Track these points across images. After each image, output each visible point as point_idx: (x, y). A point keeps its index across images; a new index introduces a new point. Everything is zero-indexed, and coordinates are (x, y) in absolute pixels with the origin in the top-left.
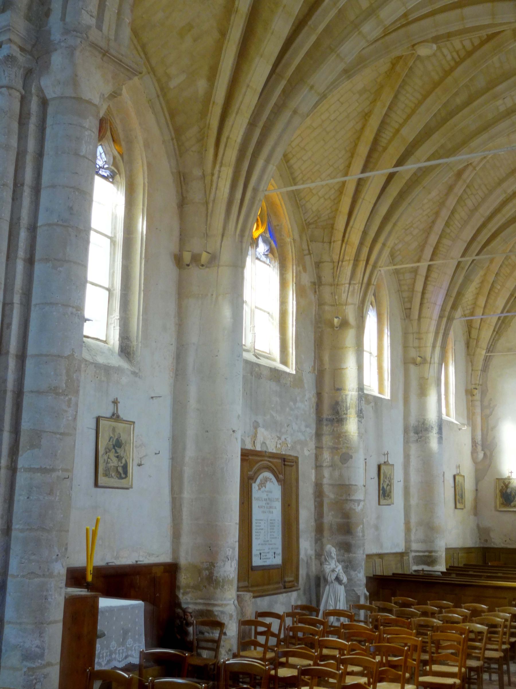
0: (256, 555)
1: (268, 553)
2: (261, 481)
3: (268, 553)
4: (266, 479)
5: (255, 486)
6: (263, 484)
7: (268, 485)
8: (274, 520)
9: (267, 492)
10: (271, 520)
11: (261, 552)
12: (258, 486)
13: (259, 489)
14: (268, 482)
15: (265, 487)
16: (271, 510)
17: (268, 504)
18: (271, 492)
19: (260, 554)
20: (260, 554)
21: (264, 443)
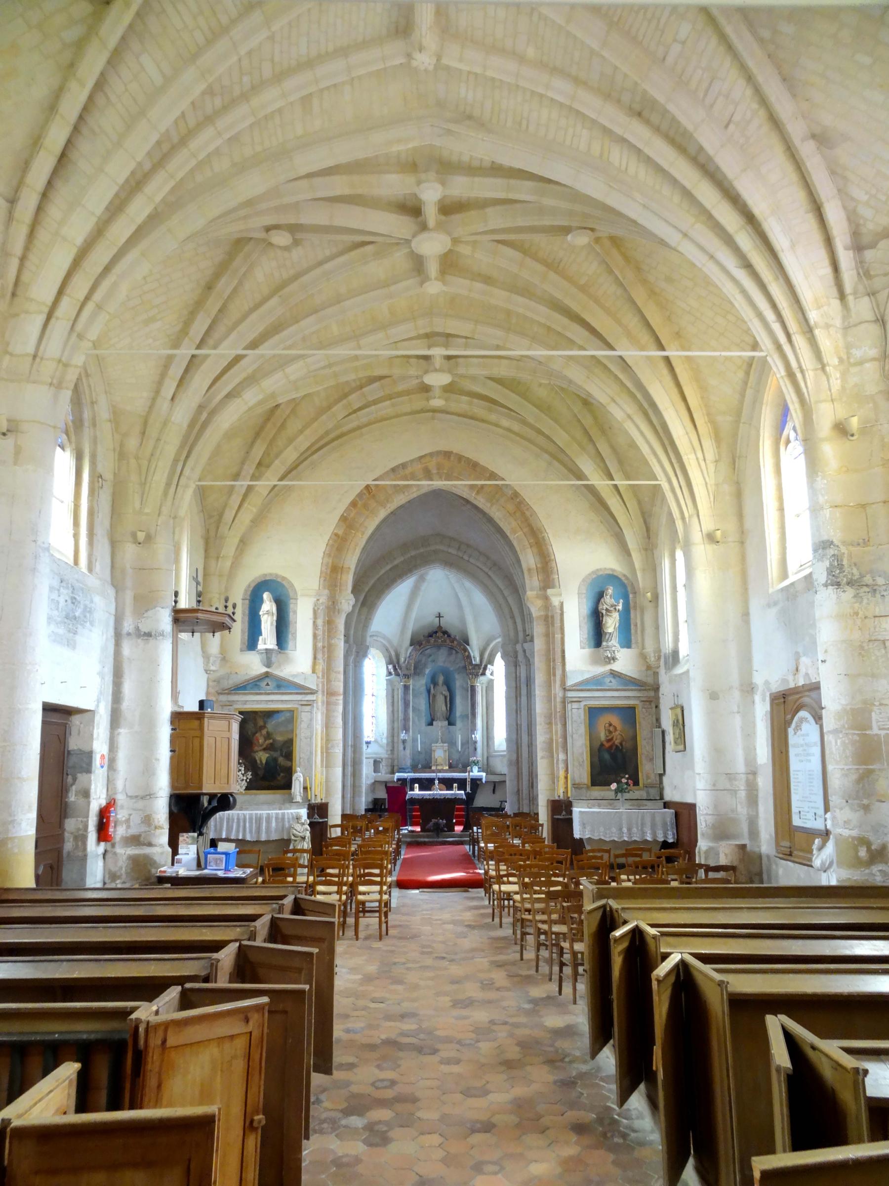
0: (795, 813)
1: (808, 812)
2: (796, 723)
3: (808, 812)
4: (802, 720)
5: (791, 731)
6: (798, 728)
7: (805, 726)
8: (813, 771)
9: (803, 735)
10: (809, 771)
11: (801, 810)
12: (794, 730)
13: (795, 733)
14: (804, 723)
15: (801, 729)
16: (809, 758)
17: (805, 750)
18: (807, 735)
19: (800, 812)
20: (800, 812)
21: (807, 674)
